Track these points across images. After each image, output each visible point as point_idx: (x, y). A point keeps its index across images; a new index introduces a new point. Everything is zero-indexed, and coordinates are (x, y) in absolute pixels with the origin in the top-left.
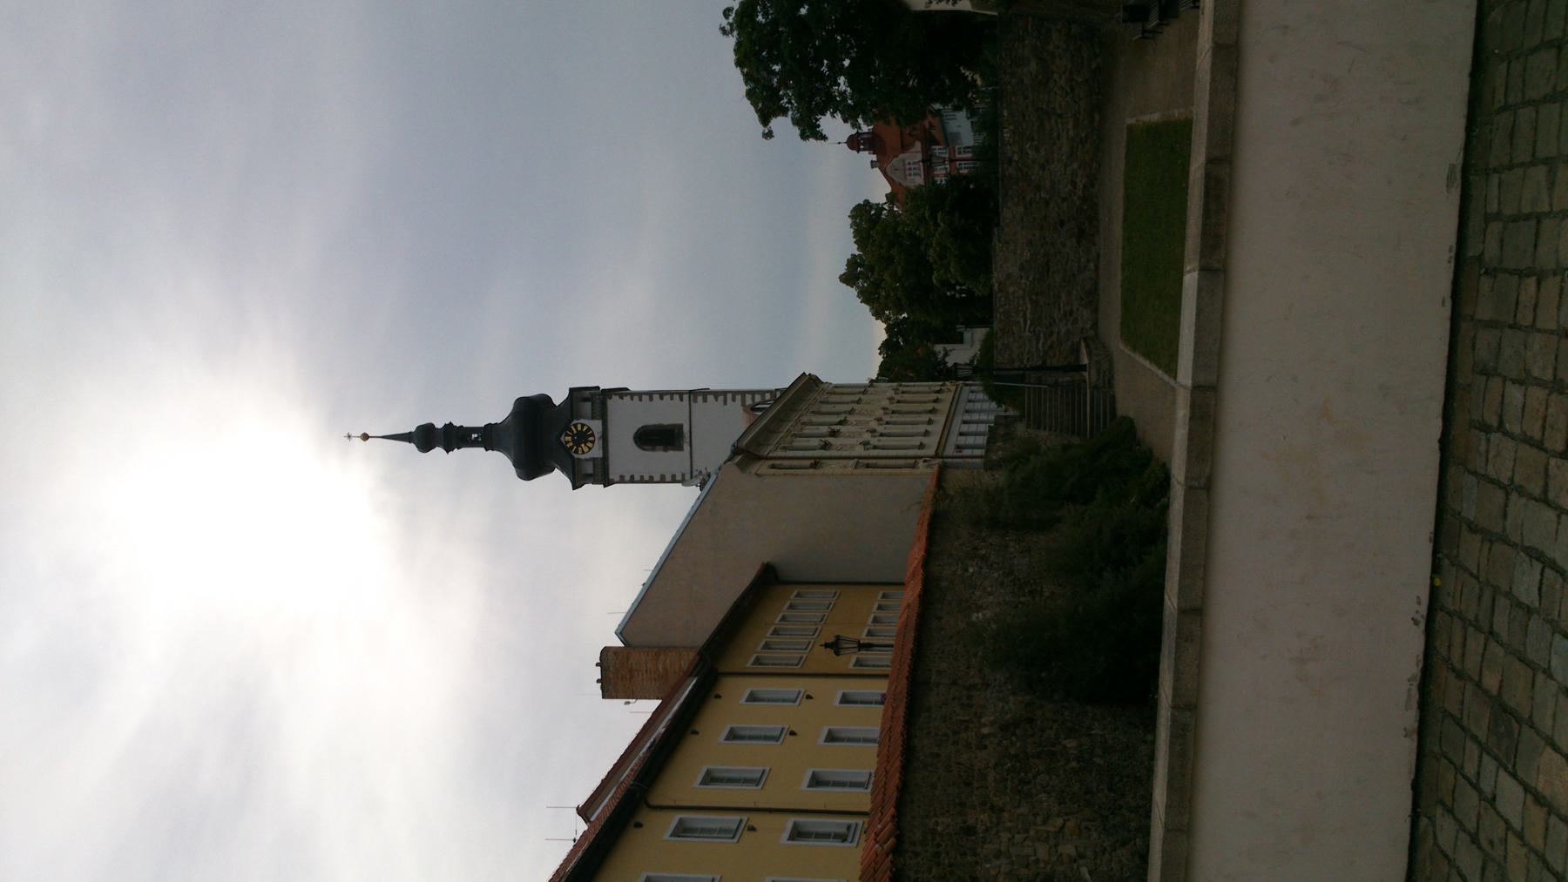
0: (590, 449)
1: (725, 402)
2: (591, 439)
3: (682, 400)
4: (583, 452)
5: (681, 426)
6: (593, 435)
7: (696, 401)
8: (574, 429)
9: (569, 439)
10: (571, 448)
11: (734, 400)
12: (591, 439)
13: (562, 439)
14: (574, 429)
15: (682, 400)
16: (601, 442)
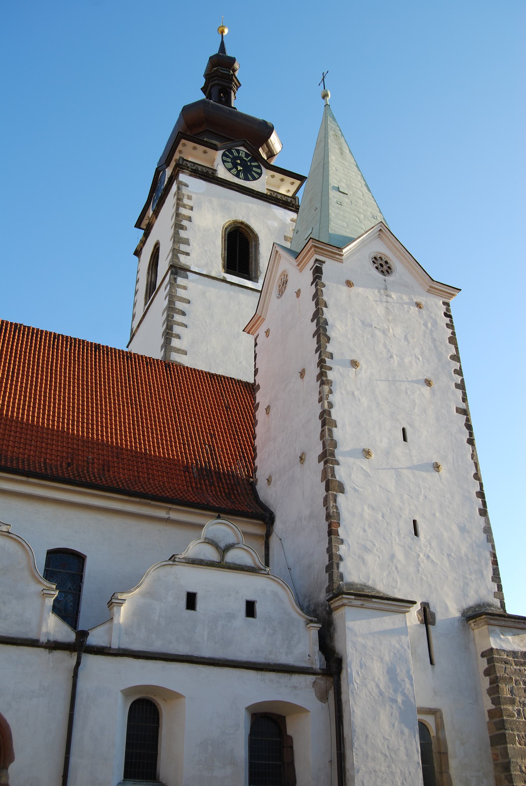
0: (229, 170)
4: (224, 161)
6: (246, 179)
12: (242, 175)
13: (241, 148)
14: (253, 164)
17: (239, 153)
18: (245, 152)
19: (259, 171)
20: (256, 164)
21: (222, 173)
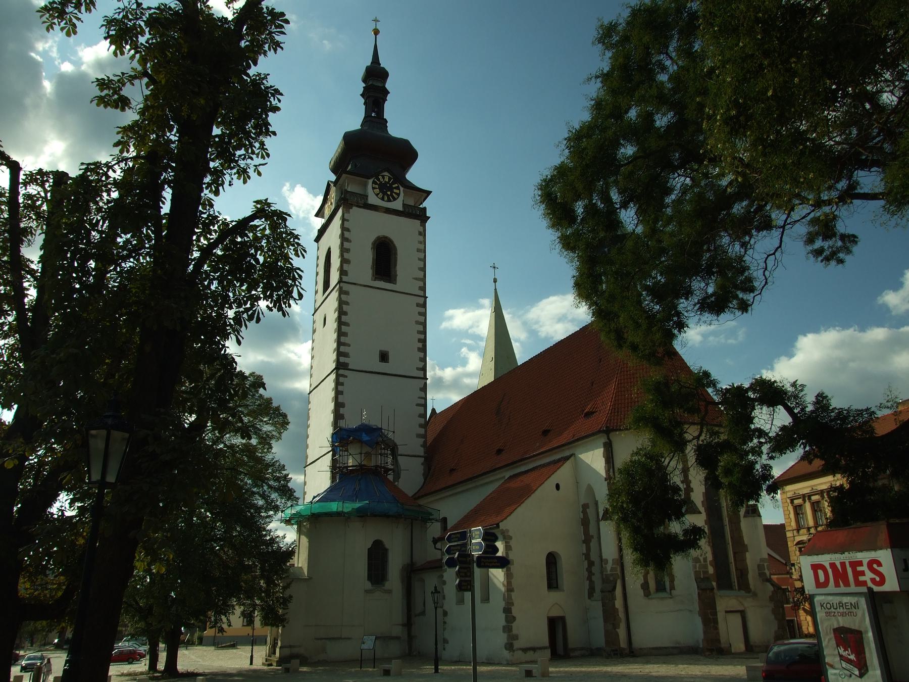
0: (377, 195)
2: (386, 198)
4: (374, 188)
6: (389, 200)
9: (387, 179)
10: (379, 180)
12: (386, 198)
13: (386, 174)
17: (384, 179)
18: (389, 177)
19: (398, 191)
20: (396, 185)
21: (373, 199)
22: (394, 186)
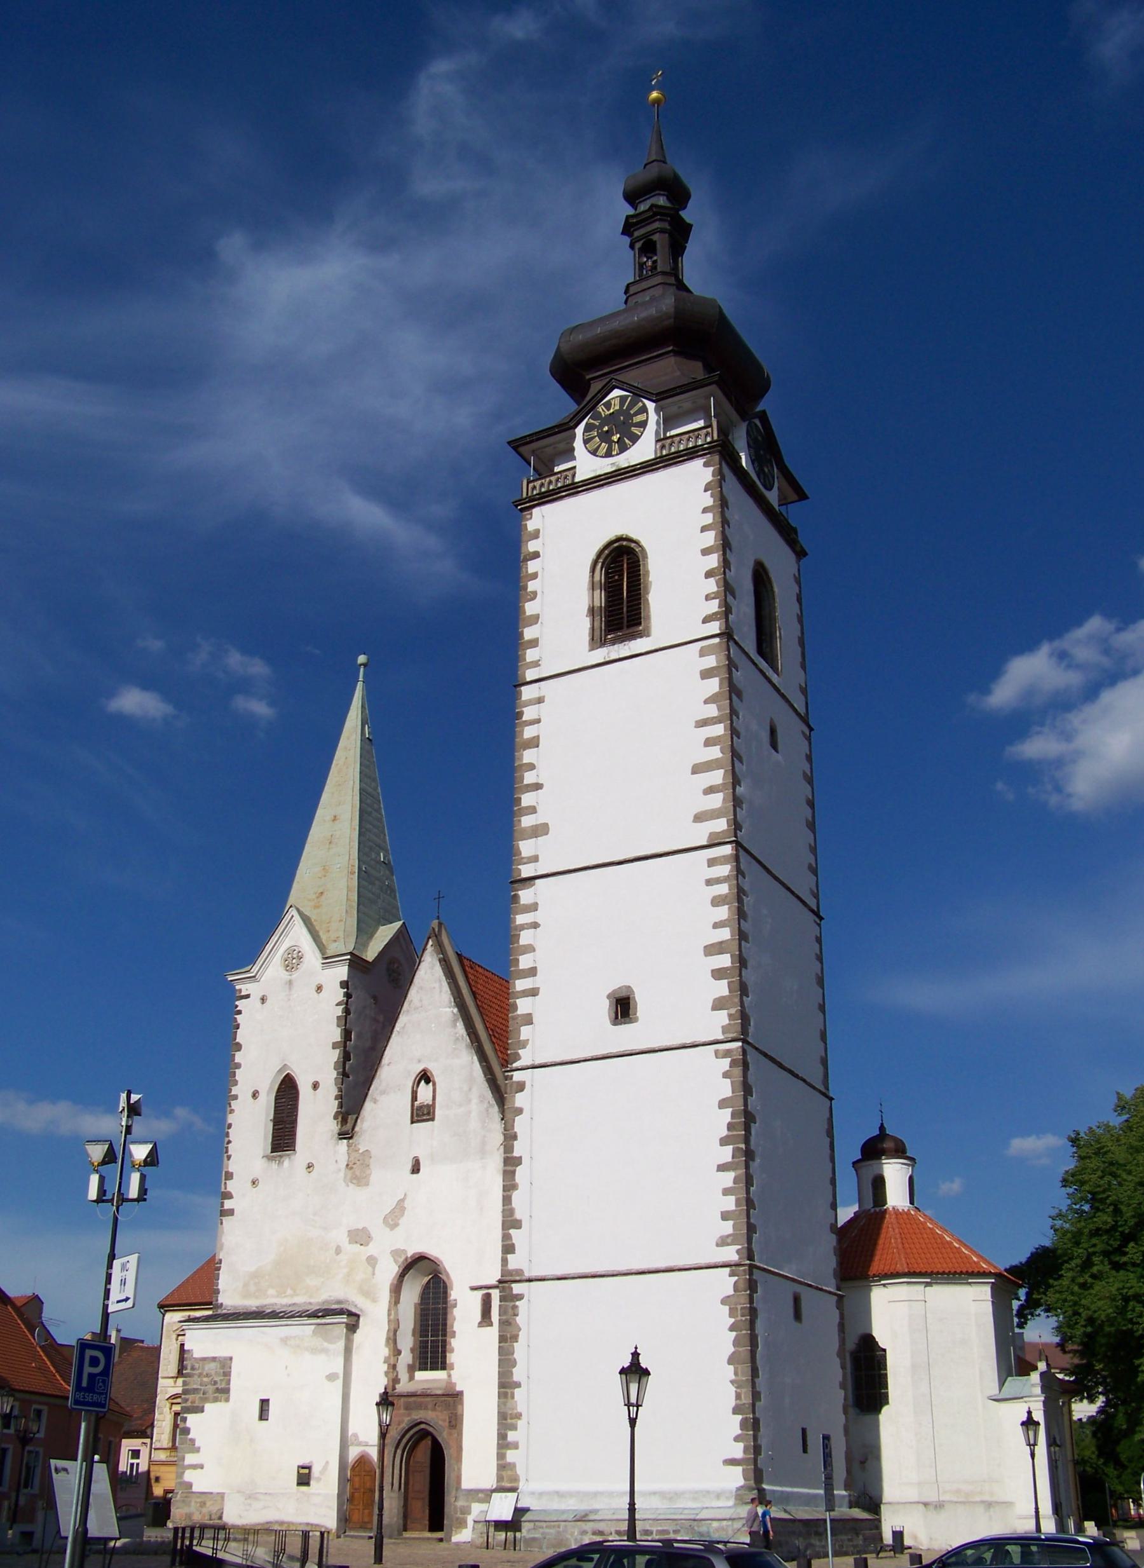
0: (594, 453)
1: (703, 723)
3: (706, 620)
5: (645, 633)
6: (623, 449)
7: (703, 653)
8: (636, 409)
10: (597, 416)
11: (709, 742)
15: (706, 620)
16: (609, 469)
20: (640, 404)
22: (632, 412)
